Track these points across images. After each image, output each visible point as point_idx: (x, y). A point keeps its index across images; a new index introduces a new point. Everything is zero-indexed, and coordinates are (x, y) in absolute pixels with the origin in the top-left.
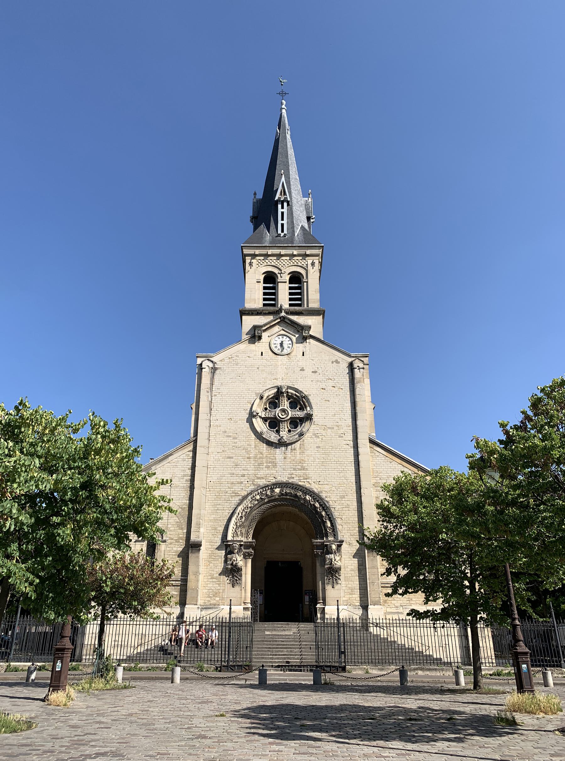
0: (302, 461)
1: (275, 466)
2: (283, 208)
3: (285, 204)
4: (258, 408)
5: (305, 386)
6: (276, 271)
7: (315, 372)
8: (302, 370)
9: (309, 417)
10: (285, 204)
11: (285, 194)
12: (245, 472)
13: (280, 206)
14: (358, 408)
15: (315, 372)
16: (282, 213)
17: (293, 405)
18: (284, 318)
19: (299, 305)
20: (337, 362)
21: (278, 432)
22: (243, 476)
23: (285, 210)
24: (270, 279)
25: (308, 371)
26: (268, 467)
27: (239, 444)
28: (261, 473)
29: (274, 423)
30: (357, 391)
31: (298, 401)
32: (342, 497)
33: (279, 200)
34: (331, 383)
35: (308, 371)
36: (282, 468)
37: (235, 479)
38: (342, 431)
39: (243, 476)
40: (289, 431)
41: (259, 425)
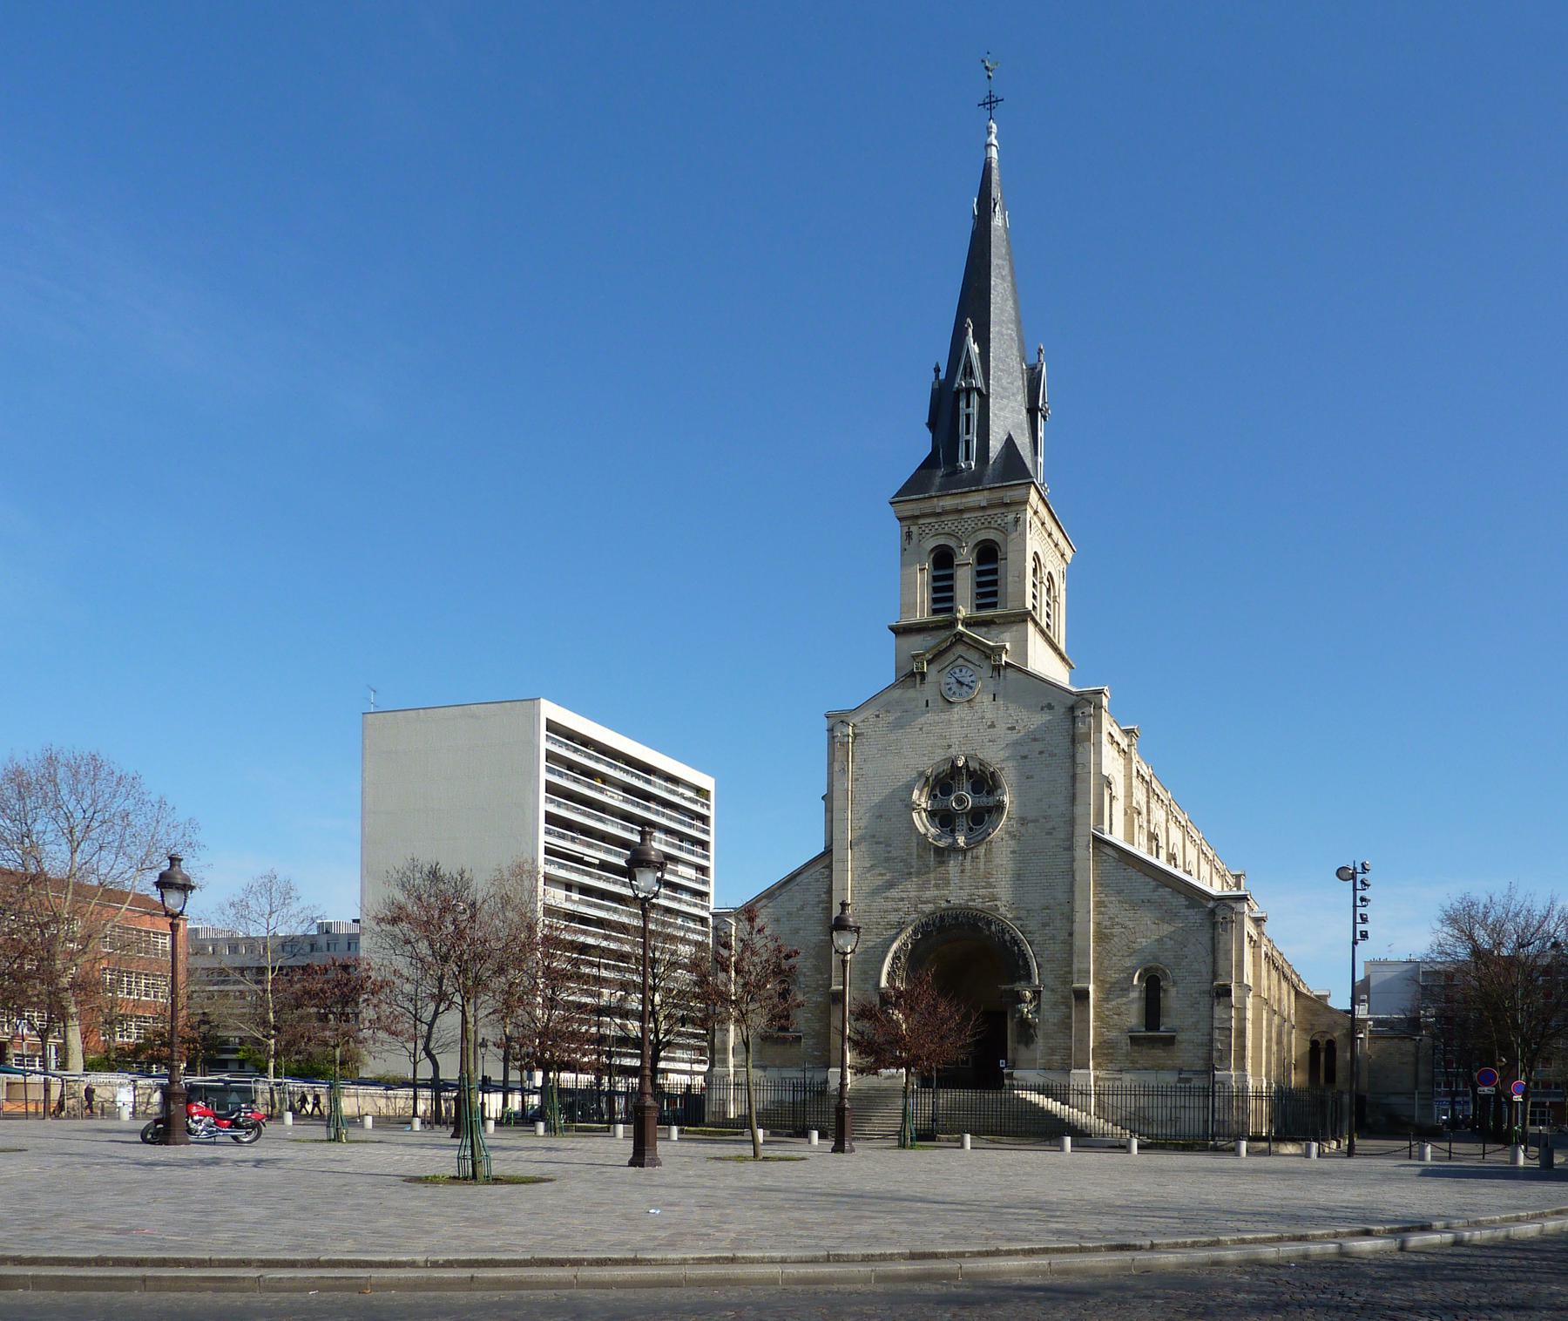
0: (988, 874)
1: (947, 883)
2: (968, 406)
3: (975, 399)
4: (920, 798)
5: (995, 756)
6: (952, 543)
7: (1013, 728)
8: (992, 726)
9: (1000, 807)
10: (975, 399)
11: (971, 374)
12: (904, 895)
13: (963, 404)
14: (1078, 785)
15: (1013, 728)
16: (968, 416)
17: (976, 789)
18: (962, 634)
19: (994, 605)
20: (1050, 707)
21: (953, 831)
22: (902, 899)
23: (974, 410)
24: (943, 559)
25: (1001, 728)
26: (937, 886)
27: (894, 854)
28: (928, 894)
29: (943, 818)
30: (1079, 759)
31: (984, 781)
32: (1045, 925)
33: (959, 391)
34: (1038, 746)
35: (1001, 728)
36: (956, 889)
37: (890, 905)
38: (1049, 825)
39: (902, 899)
40: (971, 829)
41: (921, 822)
